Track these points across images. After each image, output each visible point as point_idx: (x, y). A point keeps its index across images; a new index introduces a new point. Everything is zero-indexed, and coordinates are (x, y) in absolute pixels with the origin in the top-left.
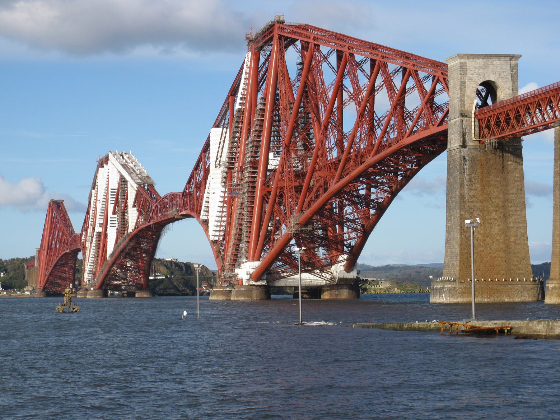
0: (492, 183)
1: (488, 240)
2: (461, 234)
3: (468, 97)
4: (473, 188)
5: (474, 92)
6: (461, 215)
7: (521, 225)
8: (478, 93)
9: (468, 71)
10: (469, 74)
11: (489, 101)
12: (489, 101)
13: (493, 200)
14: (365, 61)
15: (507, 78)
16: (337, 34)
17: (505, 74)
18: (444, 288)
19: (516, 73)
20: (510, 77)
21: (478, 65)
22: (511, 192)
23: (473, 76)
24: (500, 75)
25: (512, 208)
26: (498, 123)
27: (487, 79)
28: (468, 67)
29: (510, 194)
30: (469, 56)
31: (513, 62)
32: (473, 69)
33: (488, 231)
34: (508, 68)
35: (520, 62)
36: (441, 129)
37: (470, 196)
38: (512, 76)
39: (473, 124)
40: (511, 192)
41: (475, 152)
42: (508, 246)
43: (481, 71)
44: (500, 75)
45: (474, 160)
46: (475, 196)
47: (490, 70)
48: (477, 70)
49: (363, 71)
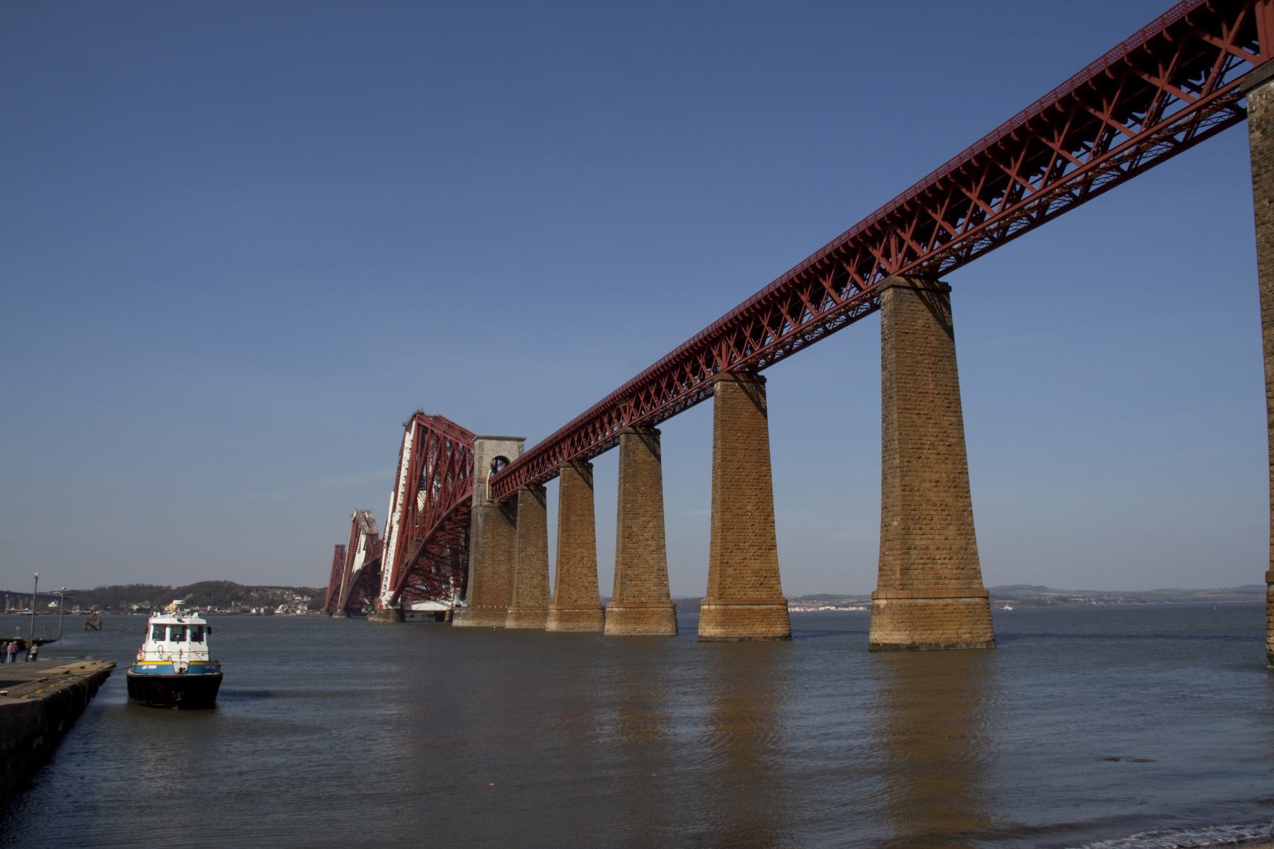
1: (496, 577)
10: (485, 451)
27: (500, 455)
41: (488, 510)
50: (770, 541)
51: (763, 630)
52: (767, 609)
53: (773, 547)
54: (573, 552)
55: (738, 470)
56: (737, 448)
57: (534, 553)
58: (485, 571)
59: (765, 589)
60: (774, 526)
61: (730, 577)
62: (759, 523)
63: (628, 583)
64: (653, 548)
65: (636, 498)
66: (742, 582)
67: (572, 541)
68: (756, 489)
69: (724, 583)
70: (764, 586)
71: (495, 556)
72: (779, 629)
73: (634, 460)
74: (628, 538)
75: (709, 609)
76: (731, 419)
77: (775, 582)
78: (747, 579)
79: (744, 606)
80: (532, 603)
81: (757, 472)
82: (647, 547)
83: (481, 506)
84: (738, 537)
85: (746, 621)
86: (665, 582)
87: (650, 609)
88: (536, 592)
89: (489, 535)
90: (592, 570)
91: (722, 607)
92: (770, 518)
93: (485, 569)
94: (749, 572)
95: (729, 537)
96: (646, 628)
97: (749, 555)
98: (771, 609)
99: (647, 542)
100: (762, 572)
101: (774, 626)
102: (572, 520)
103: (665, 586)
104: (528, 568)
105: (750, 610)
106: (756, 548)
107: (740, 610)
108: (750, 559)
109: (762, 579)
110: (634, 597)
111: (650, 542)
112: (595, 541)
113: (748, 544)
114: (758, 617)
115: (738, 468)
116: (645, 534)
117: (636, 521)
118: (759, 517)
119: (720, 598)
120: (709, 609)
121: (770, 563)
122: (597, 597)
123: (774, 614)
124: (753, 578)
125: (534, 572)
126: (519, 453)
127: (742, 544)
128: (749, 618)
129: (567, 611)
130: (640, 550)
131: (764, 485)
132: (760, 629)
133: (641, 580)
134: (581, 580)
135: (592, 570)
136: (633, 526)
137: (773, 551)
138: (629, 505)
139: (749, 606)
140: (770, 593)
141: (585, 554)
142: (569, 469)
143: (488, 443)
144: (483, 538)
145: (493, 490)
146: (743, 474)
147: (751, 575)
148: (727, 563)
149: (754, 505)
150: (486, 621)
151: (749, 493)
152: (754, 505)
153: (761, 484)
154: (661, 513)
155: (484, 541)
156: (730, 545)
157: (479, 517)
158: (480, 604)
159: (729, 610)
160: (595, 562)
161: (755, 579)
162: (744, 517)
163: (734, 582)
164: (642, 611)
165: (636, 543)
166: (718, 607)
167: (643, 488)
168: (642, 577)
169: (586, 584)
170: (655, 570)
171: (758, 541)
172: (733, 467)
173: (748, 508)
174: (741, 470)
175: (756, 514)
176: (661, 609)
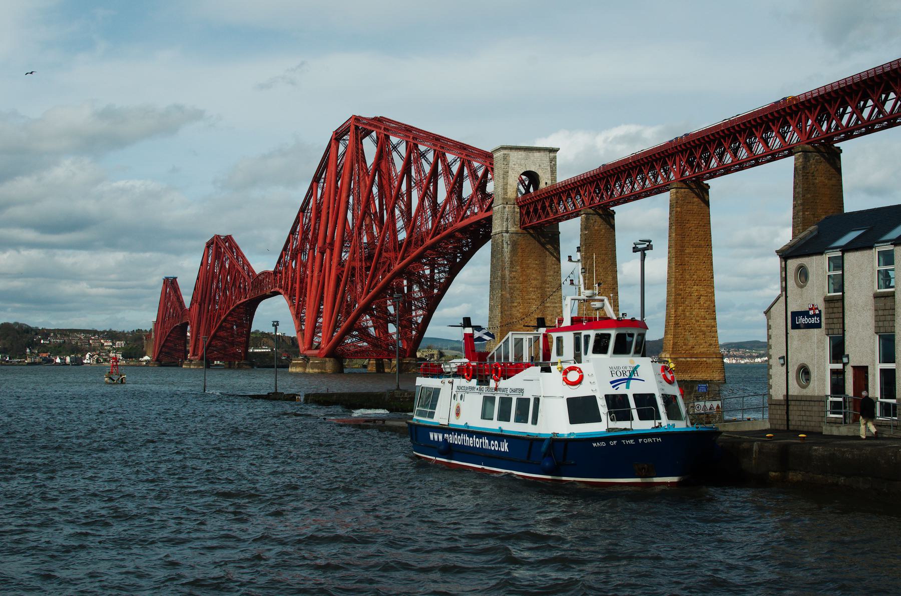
0: (531, 265)
2: (502, 313)
3: (510, 185)
4: (514, 269)
6: (502, 295)
7: (557, 305)
8: (522, 182)
10: (511, 164)
11: (531, 190)
12: (531, 190)
13: (532, 282)
14: (429, 150)
16: (406, 125)
19: (555, 165)
20: (549, 168)
22: (548, 274)
24: (540, 166)
25: (549, 290)
26: (536, 211)
28: (511, 158)
29: (548, 276)
30: (511, 148)
31: (552, 155)
35: (558, 153)
36: (488, 214)
38: (551, 168)
40: (548, 274)
41: (515, 237)
43: (523, 162)
45: (515, 245)
49: (427, 160)
54: (688, 290)
67: (687, 277)
73: (813, 184)
83: (507, 232)
89: (518, 268)
93: (514, 309)
102: (686, 251)
122: (716, 344)
129: (684, 359)
134: (698, 323)
141: (702, 293)
142: (683, 190)
144: (511, 272)
145: (521, 213)
157: (505, 246)
169: (703, 328)
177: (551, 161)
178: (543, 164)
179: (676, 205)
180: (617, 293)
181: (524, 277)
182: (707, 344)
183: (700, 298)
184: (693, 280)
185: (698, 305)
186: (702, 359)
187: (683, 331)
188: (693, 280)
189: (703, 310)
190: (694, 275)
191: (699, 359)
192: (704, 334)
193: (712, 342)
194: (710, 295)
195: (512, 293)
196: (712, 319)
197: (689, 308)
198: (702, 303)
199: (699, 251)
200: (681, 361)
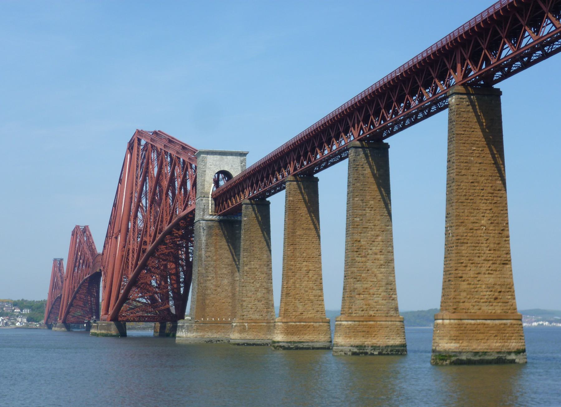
1: (219, 290)
3: (207, 182)
4: (209, 250)
5: (212, 178)
9: (208, 163)
15: (238, 169)
17: (236, 165)
18: (184, 325)
21: (215, 159)
23: (212, 167)
24: (232, 166)
27: (222, 169)
28: (208, 160)
32: (212, 161)
33: (219, 283)
34: (238, 161)
37: (206, 256)
39: (210, 202)
42: (234, 295)
43: (218, 163)
44: (232, 166)
46: (209, 257)
47: (225, 162)
48: (214, 162)
50: (505, 256)
51: (498, 344)
52: (502, 324)
53: (507, 262)
54: (298, 265)
55: (473, 184)
56: (471, 162)
57: (258, 266)
58: (208, 284)
59: (500, 304)
60: (509, 241)
61: (464, 291)
62: (494, 237)
63: (357, 296)
64: (382, 262)
65: (364, 212)
66: (477, 296)
67: (298, 254)
68: (491, 203)
69: (458, 297)
70: (498, 300)
71: (218, 270)
72: (514, 344)
74: (357, 252)
75: (443, 324)
76: (466, 133)
77: (509, 297)
78: (482, 294)
79: (478, 321)
80: (256, 316)
81: (491, 187)
82: (376, 261)
84: (472, 252)
85: (481, 336)
86: (393, 296)
87: (378, 322)
88: (260, 305)
90: (318, 283)
91: (456, 321)
92: (505, 233)
93: (208, 282)
94: (484, 286)
95: (464, 252)
96: (374, 341)
97: (483, 270)
98: (505, 324)
99: (376, 256)
100: (496, 287)
101: (509, 341)
102: (297, 233)
103: (393, 300)
104: (252, 281)
105: (485, 324)
106: (491, 262)
107: (474, 324)
108: (485, 274)
109: (496, 294)
110: (362, 311)
111: (379, 256)
112: (320, 255)
113: (483, 258)
114: (492, 332)
115: (472, 182)
116: (374, 248)
117: (365, 235)
118: (494, 232)
119: (454, 313)
120: (443, 324)
121: (504, 278)
122: (323, 312)
123: (510, 329)
124: (488, 293)
125: (258, 285)
126: (242, 167)
127: (476, 259)
128: (483, 333)
129: (293, 323)
130: (369, 264)
131: (499, 199)
132: (494, 344)
133: (369, 294)
135: (318, 283)
136: (362, 240)
137: (508, 266)
138: (358, 219)
139: (484, 321)
140: (505, 308)
141: (311, 268)
143: (210, 159)
144: (206, 252)
146: (478, 188)
147: (485, 290)
148: (461, 277)
149: (489, 220)
150: (210, 334)
151: (483, 206)
152: (489, 220)
153: (495, 198)
154: (389, 227)
155: (207, 255)
156: (464, 260)
158: (204, 317)
159: (463, 324)
160: (320, 275)
161: (490, 293)
162: (479, 232)
163: (468, 297)
164: (370, 325)
165: (365, 257)
166: (452, 321)
167: (372, 202)
168: (371, 291)
169: (311, 297)
170: (384, 283)
171: (493, 255)
172: (467, 181)
173: (483, 222)
174: (476, 184)
175: (491, 228)
176: (390, 323)
177: (242, 162)
178: (235, 164)
179: (289, 195)
180: (271, 268)
181: (218, 256)
182: (315, 311)
183: (308, 272)
184: (303, 257)
185: (307, 278)
186: (310, 324)
187: (293, 300)
188: (303, 257)
189: (311, 282)
190: (303, 253)
191: (307, 323)
192: (312, 302)
193: (319, 309)
194: (318, 269)
195: (207, 269)
196: (319, 290)
197: (299, 280)
198: (310, 276)
199: (309, 233)
200: (291, 325)
